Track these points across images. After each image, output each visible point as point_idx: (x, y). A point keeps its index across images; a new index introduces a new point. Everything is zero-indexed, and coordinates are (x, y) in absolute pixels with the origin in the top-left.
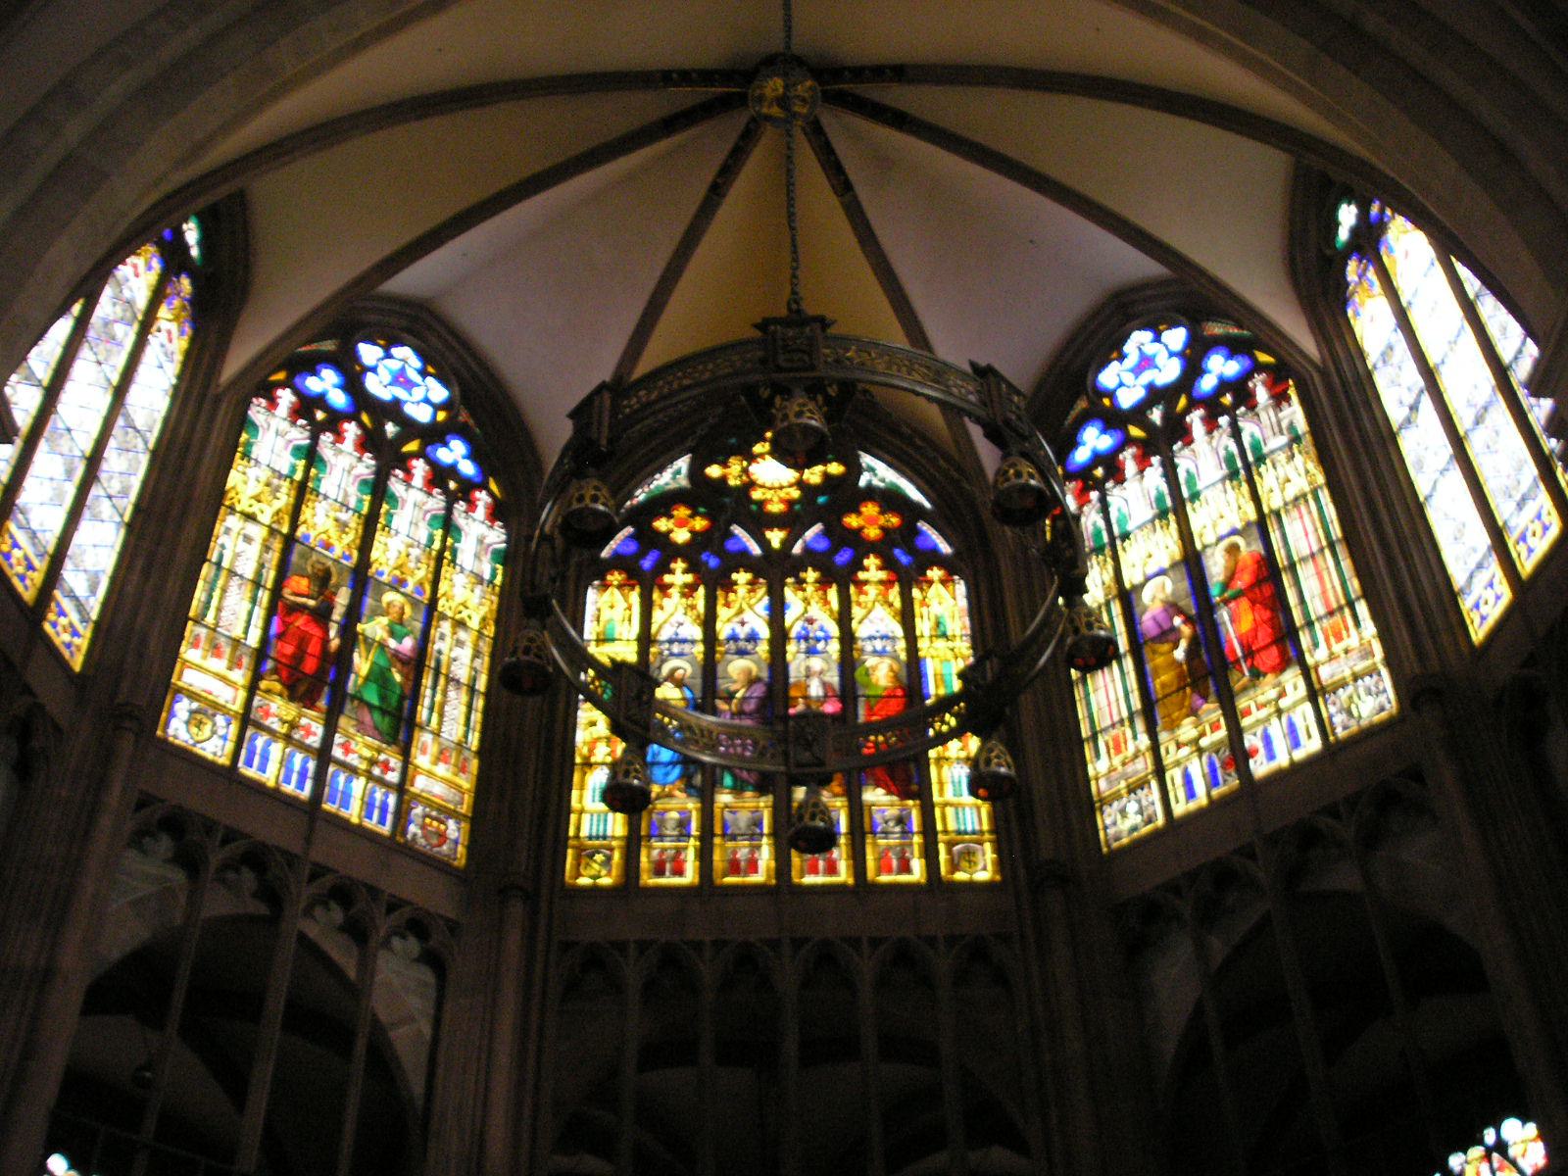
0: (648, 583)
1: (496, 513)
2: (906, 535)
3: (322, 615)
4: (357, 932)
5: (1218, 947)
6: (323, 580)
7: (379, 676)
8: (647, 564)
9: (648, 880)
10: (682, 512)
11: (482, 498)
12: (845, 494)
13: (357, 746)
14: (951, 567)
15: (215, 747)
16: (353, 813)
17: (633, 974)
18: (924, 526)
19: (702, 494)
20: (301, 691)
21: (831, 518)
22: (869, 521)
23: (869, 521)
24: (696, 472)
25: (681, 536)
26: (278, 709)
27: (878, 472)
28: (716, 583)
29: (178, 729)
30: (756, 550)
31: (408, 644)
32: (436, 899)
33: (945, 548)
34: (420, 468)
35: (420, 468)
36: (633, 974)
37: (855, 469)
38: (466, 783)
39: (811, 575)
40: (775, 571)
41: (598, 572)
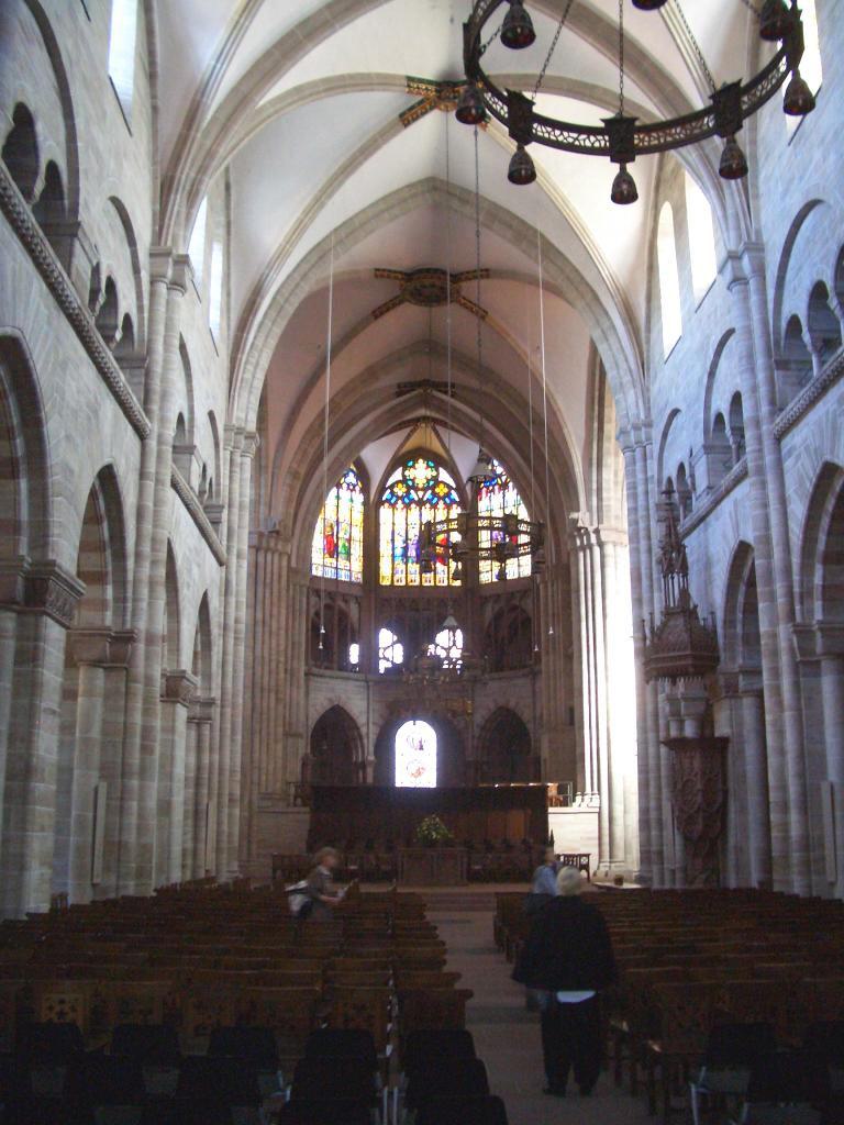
0: (393, 506)
1: (362, 491)
2: (448, 495)
3: (333, 535)
4: (346, 601)
5: (497, 608)
6: (331, 526)
7: (344, 546)
8: (393, 501)
9: (396, 584)
10: (400, 485)
11: (357, 488)
12: (435, 479)
13: (342, 563)
14: (459, 504)
15: (319, 574)
16: (343, 579)
17: (393, 603)
18: (453, 492)
19: (404, 480)
20: (332, 556)
21: (433, 488)
22: (441, 490)
23: (441, 490)
24: (404, 476)
25: (400, 494)
26: (330, 561)
27: (444, 476)
28: (407, 506)
29: (314, 573)
30: (416, 499)
31: (347, 536)
32: (357, 592)
33: (458, 500)
34: (345, 486)
35: (345, 486)
36: (393, 603)
37: (438, 474)
38: (361, 564)
39: (428, 505)
40: (421, 503)
41: (383, 503)
